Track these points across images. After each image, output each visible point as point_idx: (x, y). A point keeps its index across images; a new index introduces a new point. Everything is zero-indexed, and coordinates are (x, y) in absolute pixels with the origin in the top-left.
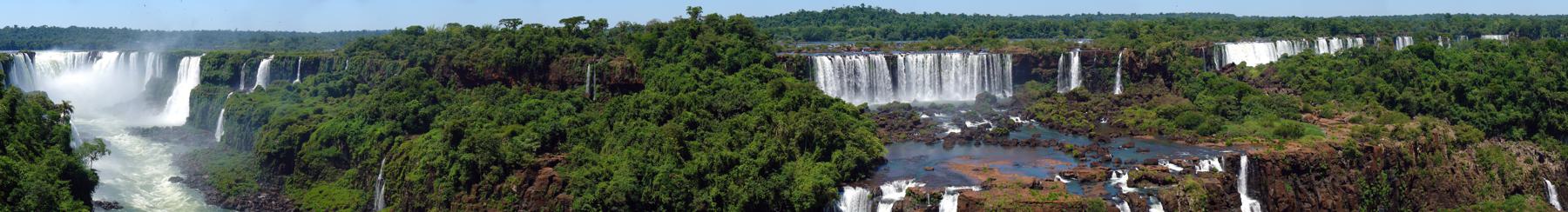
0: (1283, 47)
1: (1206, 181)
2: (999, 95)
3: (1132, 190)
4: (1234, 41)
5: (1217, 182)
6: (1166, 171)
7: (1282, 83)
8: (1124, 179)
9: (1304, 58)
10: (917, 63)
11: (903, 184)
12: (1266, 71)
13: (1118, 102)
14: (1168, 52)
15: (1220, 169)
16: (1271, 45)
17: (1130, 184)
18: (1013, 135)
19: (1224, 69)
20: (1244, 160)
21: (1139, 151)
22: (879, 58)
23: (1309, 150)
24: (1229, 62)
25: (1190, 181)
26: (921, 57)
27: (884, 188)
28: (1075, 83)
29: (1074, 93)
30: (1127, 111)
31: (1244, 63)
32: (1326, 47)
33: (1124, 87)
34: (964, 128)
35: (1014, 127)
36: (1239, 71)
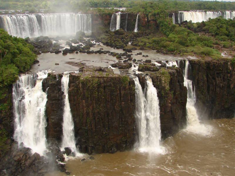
1: (170, 71)
2: (85, 32)
3: (140, 73)
4: (188, 11)
6: (155, 65)
7: (206, 31)
8: (137, 68)
9: (218, 20)
11: (46, 71)
12: (201, 27)
13: (137, 35)
14: (158, 14)
15: (177, 66)
16: (204, 13)
17: (139, 70)
18: (92, 49)
19: (182, 23)
20: (187, 63)
21: (143, 56)
22: (33, 16)
23: (215, 61)
24: (185, 20)
25: (163, 70)
28: (118, 27)
29: (118, 31)
31: (191, 21)
33: (138, 29)
34: (71, 46)
35: (92, 45)
36: (188, 25)
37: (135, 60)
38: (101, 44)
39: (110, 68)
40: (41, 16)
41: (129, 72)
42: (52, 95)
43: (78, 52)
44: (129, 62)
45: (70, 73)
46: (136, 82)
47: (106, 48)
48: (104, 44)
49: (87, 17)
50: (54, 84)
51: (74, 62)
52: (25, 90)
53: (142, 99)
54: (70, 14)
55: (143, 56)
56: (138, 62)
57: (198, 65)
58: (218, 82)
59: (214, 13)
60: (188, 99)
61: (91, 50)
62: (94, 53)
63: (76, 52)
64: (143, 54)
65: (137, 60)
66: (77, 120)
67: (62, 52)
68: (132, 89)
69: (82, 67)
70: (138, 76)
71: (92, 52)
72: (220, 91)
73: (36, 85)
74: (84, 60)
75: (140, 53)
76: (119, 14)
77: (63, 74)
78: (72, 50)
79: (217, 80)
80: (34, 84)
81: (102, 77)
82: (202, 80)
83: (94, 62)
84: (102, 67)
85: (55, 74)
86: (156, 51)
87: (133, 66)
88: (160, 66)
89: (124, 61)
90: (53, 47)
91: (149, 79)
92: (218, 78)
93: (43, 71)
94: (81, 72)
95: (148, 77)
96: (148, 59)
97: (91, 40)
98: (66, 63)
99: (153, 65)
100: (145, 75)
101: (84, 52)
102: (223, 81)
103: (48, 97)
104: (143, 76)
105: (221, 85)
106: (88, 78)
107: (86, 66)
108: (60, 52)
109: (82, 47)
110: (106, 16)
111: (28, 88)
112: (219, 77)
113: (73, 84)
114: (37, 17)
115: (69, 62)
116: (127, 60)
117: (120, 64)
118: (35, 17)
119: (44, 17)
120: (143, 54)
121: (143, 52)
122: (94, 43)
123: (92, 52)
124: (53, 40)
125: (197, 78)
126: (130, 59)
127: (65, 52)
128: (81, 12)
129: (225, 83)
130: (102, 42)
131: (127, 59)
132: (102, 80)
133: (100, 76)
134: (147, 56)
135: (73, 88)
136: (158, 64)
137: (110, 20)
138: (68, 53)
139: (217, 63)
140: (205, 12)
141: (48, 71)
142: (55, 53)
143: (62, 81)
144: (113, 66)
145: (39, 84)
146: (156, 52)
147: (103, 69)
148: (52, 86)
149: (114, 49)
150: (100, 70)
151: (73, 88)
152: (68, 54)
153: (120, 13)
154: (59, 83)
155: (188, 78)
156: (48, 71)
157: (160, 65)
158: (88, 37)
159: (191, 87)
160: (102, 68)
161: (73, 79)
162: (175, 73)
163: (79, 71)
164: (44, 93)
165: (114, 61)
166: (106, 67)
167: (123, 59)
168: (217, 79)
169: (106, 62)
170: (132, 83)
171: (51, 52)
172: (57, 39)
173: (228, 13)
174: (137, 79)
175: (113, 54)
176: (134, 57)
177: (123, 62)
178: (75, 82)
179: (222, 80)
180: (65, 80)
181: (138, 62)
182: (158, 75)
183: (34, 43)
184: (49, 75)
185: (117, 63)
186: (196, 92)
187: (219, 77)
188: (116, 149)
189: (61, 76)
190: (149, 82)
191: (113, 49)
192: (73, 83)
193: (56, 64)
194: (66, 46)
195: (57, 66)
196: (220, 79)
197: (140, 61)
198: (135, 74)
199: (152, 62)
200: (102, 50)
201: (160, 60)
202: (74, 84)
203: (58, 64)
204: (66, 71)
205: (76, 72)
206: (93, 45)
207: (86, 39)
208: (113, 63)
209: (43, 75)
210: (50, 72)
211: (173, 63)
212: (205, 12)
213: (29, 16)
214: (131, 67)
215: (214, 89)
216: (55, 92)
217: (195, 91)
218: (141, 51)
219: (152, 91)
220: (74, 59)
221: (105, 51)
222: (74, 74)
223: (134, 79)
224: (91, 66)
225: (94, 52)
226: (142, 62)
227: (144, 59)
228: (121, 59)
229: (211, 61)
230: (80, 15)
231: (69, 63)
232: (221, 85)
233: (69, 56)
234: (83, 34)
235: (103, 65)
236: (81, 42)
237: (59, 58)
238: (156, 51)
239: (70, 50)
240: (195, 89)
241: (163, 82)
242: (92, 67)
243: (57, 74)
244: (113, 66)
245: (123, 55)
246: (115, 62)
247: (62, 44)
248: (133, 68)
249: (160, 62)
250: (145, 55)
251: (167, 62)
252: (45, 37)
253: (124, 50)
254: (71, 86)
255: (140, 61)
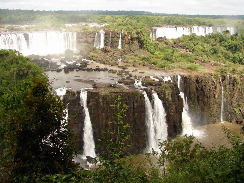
46: (145, 96)
49: (73, 35)
50: (74, 100)
53: (150, 111)
66: (97, 131)
67: (63, 70)
68: (143, 101)
70: (145, 90)
72: (208, 100)
75: (136, 70)
79: (205, 91)
81: (118, 93)
87: (136, 82)
88: (159, 81)
94: (94, 89)
106: (106, 94)
110: (91, 34)
115: (77, 80)
125: (189, 91)
133: (116, 92)
137: (94, 38)
143: (81, 97)
147: (113, 85)
154: (79, 99)
161: (91, 95)
163: (93, 88)
166: (115, 83)
169: (111, 79)
180: (84, 96)
184: (68, 92)
186: (188, 102)
189: (79, 93)
190: (155, 95)
192: (92, 98)
204: (81, 88)
215: (202, 99)
216: (76, 107)
219: (159, 103)
220: (79, 76)
250: (141, 71)
252: (36, 55)
254: (91, 101)
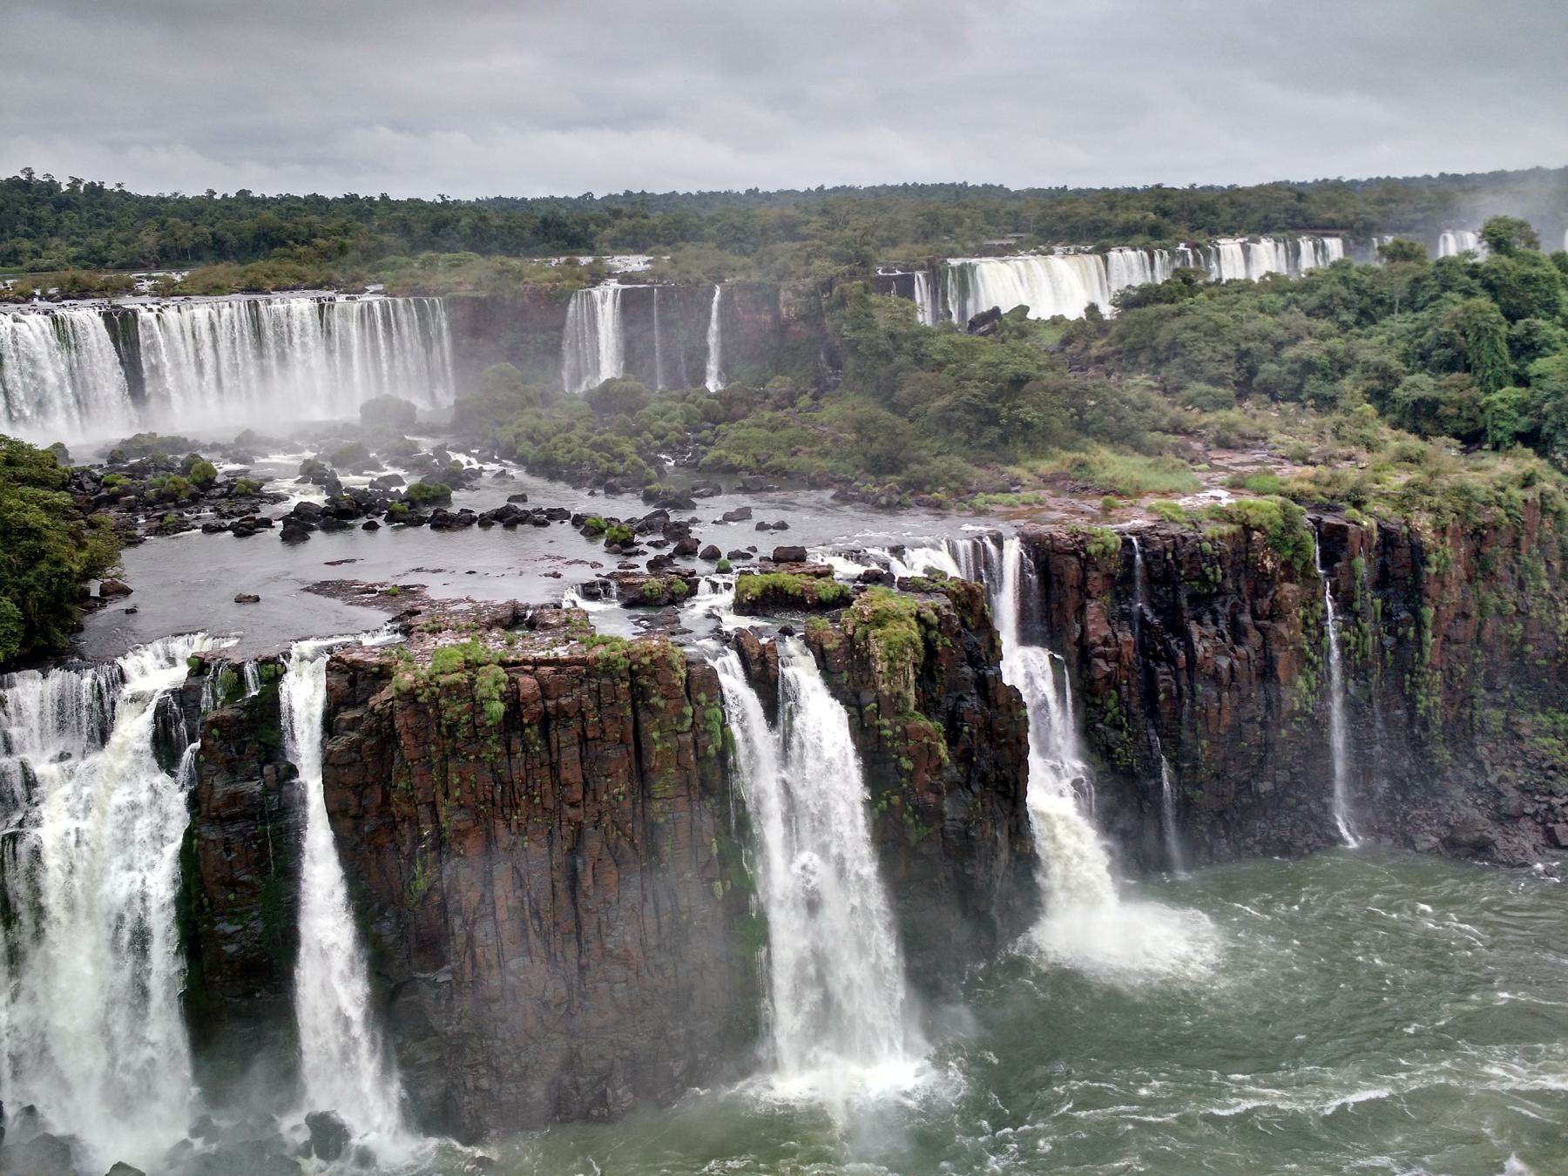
0: (1130, 267)
2: (421, 404)
3: (746, 622)
4: (1001, 252)
5: (942, 601)
8: (728, 597)
10: (181, 323)
11: (180, 647)
16: (1093, 261)
17: (740, 608)
21: (761, 527)
22: (86, 316)
23: (1174, 530)
24: (985, 308)
25: (878, 598)
26: (201, 310)
27: (129, 664)
28: (609, 367)
30: (734, 432)
32: (1243, 260)
34: (333, 487)
35: (460, 478)
37: (712, 555)
38: (515, 472)
39: (574, 603)
40: (134, 312)
41: (684, 624)
42: (221, 787)
43: (380, 521)
44: (682, 564)
45: (330, 650)
46: (724, 679)
47: (544, 494)
48: (533, 469)
51: (354, 582)
52: (43, 767)
54: (319, 300)
55: (761, 527)
56: (732, 564)
57: (1074, 559)
58: (1200, 648)
59: (1152, 257)
60: (1034, 759)
61: (454, 510)
62: (476, 525)
63: (364, 520)
64: (759, 516)
65: (724, 556)
69: (406, 609)
70: (737, 642)
71: (464, 521)
72: (1220, 699)
73: (115, 739)
74: (419, 570)
76: (610, 292)
77: (287, 656)
78: (343, 513)
79: (1196, 638)
80: (102, 734)
82: (1106, 642)
83: (475, 574)
84: (522, 601)
85: (237, 660)
86: (832, 492)
87: (703, 586)
89: (650, 565)
90: (222, 496)
91: (801, 658)
92: (1200, 623)
93: (158, 645)
95: (792, 645)
96: (786, 540)
97: (451, 449)
98: (307, 590)
99: (819, 575)
100: (775, 632)
101: (417, 522)
102: (1228, 638)
103: (194, 802)
104: (764, 641)
105: (1224, 663)
107: (431, 603)
108: (267, 523)
109: (403, 489)
111: (63, 757)
112: (1207, 618)
113: (348, 715)
114: (107, 317)
116: (671, 556)
117: (630, 580)
118: (100, 321)
119: (152, 316)
120: (759, 516)
121: (758, 504)
122: (469, 463)
123: (464, 521)
124: (216, 455)
125: (1077, 635)
126: (687, 551)
127: (299, 526)
128: (380, 287)
129: (1241, 651)
130: (521, 461)
131: (666, 552)
132: (527, 683)
134: (782, 526)
135: (355, 735)
136: (845, 569)
138: (312, 529)
139: (1185, 539)
140: (1103, 251)
141: (190, 644)
142: (230, 533)
144: (589, 592)
145: (134, 728)
146: (833, 497)
147: (529, 613)
148: (222, 734)
149: (592, 494)
150: (515, 619)
151: (355, 735)
152: (317, 536)
153: (613, 284)
154: (265, 716)
155: (1025, 638)
156: (190, 644)
157: (859, 570)
158: (430, 430)
159: (1046, 687)
160: (527, 607)
161: (351, 681)
162: (945, 612)
164: (162, 779)
165: (594, 565)
166: (547, 599)
167: (647, 551)
168: (1194, 627)
169: (552, 571)
170: (704, 683)
171: (209, 529)
172: (244, 446)
173: (1230, 247)
174: (732, 658)
175: (590, 528)
176: (705, 534)
177: (644, 569)
178: (366, 701)
179: (1222, 636)
180: (304, 695)
181: (732, 564)
182: (850, 632)
183: (97, 481)
184: (199, 667)
185: (610, 576)
187: (1207, 618)
188: (630, 1095)
190: (802, 673)
191: (584, 494)
193: (240, 600)
194: (302, 487)
195: (251, 607)
196: (1213, 629)
197: (747, 557)
198: (719, 634)
199: (810, 559)
200: (520, 506)
201: (853, 544)
202: (357, 713)
203: (257, 599)
205: (368, 641)
206: (469, 479)
207: (426, 446)
208: (588, 575)
209: (153, 673)
210: (201, 645)
211: (931, 551)
212: (1103, 251)
213: (58, 313)
214: (693, 591)
217: (1070, 709)
218: (745, 500)
219: (823, 718)
221: (540, 511)
222: (357, 656)
223: (716, 665)
224: (461, 601)
225: (474, 520)
226: (755, 559)
227: (767, 545)
228: (637, 553)
229: (1153, 528)
230: (376, 305)
231: (323, 588)
232: (1224, 663)
233: (322, 545)
234: (407, 417)
235: (532, 593)
236: (394, 464)
237: (264, 558)
238: (832, 492)
239: (325, 513)
240: (1069, 694)
241: (879, 668)
242: (465, 606)
243: (253, 654)
244: (589, 592)
245: (646, 527)
246: (598, 570)
247: (270, 479)
248: (704, 601)
249: (855, 555)
251: (898, 551)
253: (649, 498)
255: (747, 557)
